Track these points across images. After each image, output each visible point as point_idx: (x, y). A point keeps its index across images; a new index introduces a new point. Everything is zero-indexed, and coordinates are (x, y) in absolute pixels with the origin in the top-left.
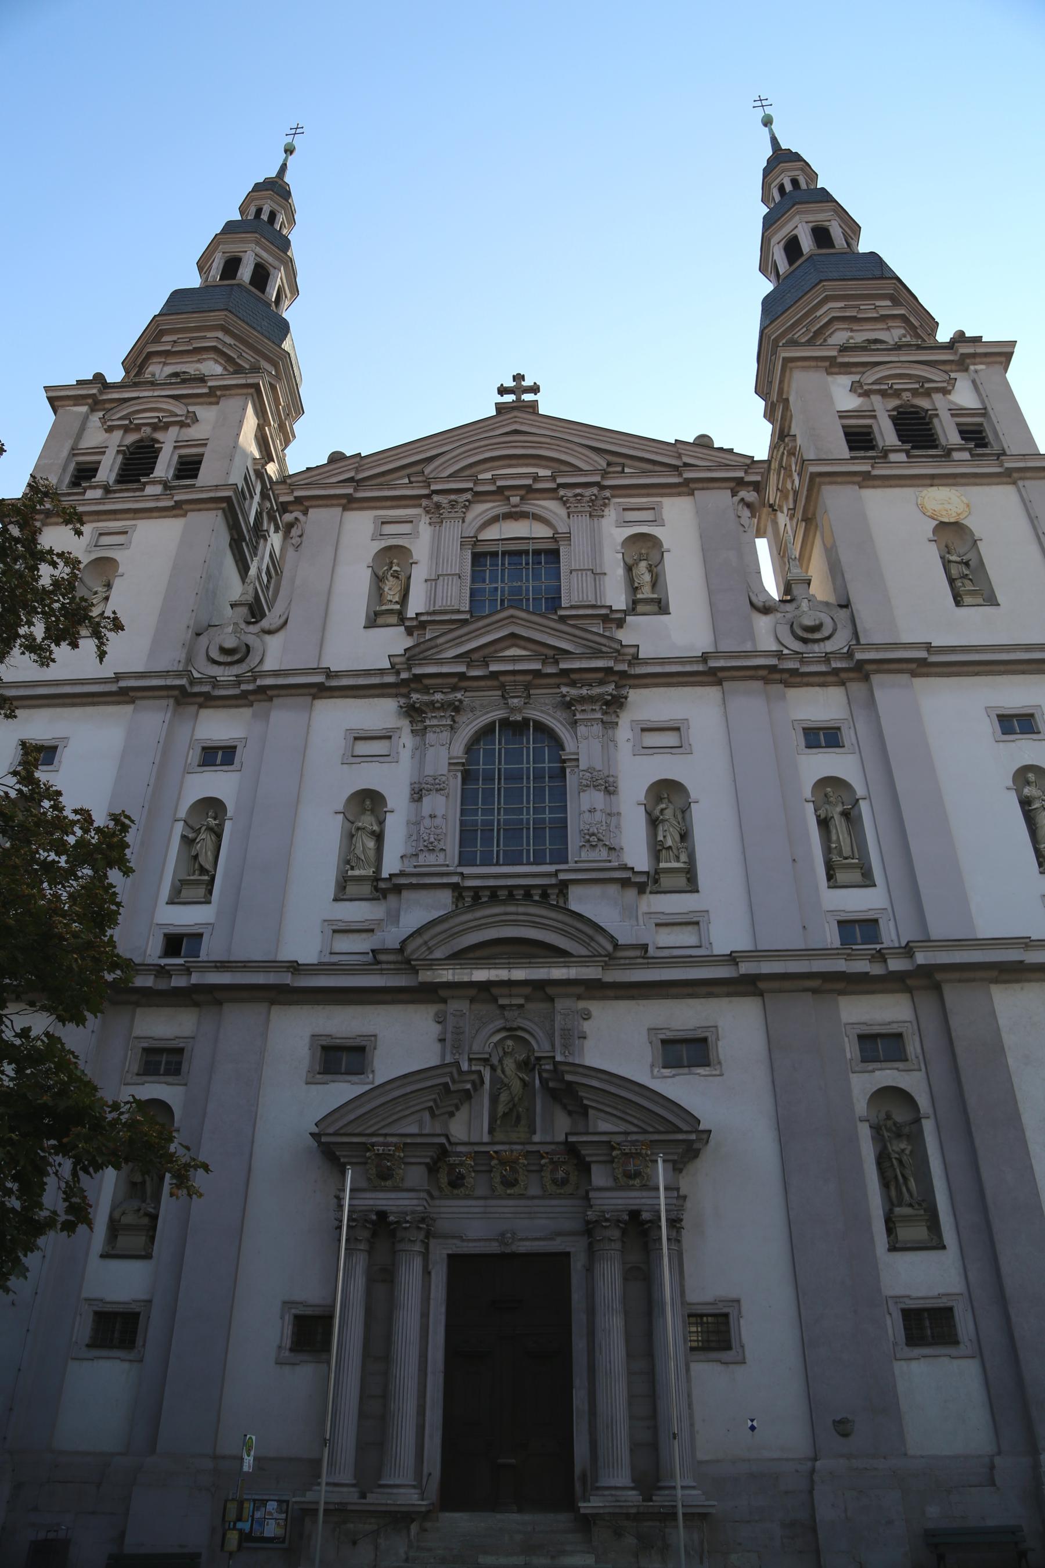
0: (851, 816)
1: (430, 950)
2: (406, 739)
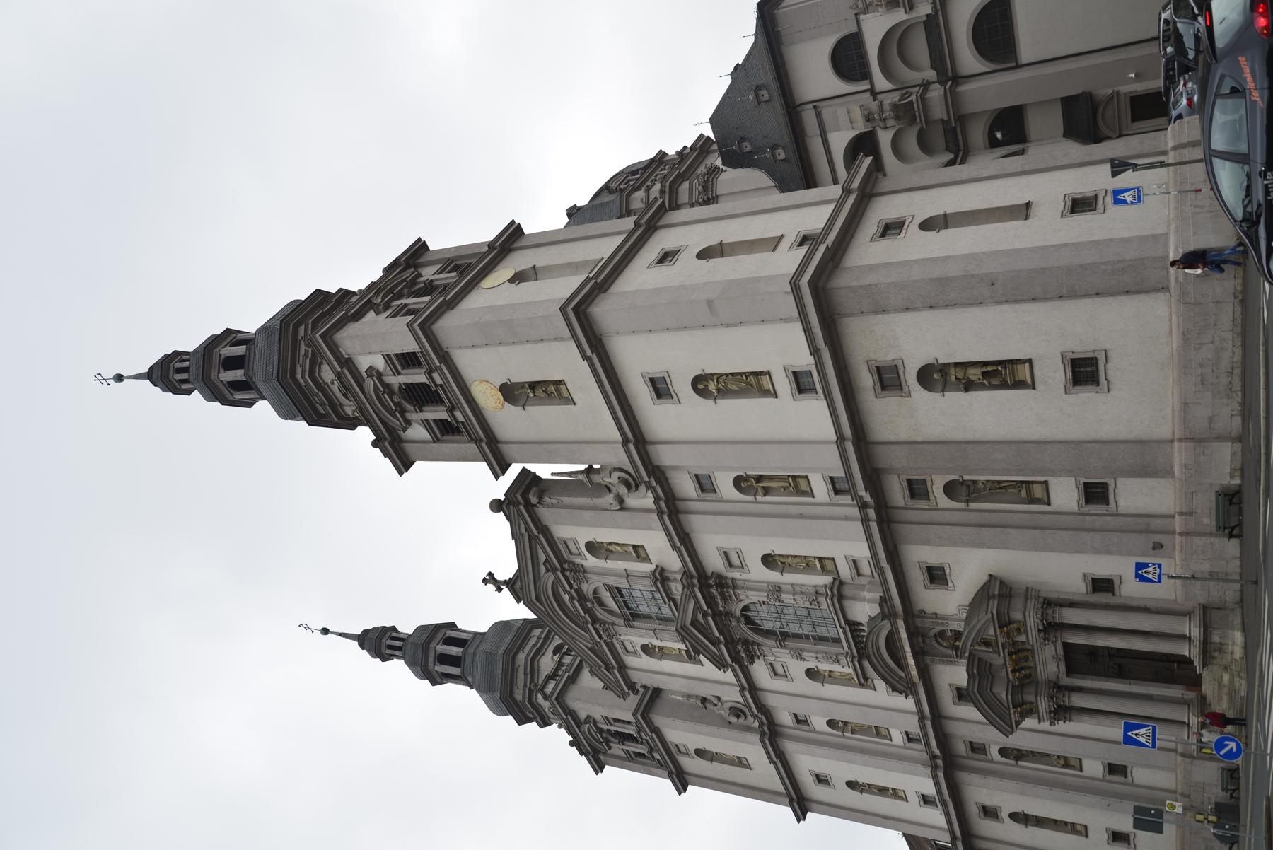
0: (759, 478)
1: (901, 678)
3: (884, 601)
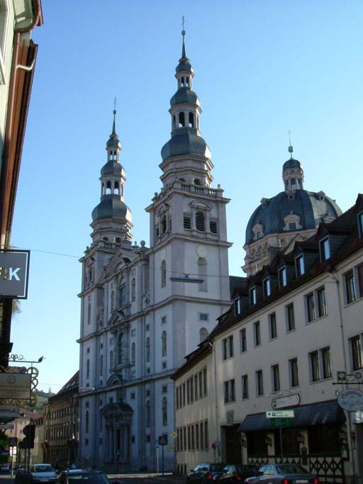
3: (125, 381)
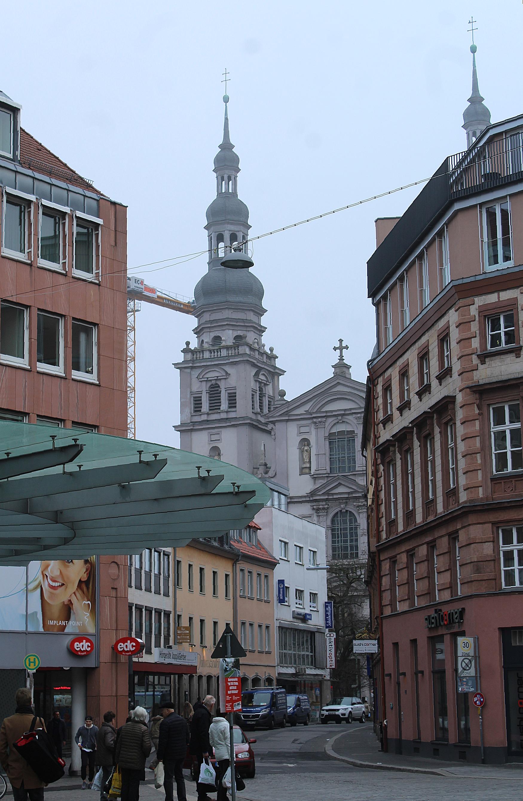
2: (315, 518)
